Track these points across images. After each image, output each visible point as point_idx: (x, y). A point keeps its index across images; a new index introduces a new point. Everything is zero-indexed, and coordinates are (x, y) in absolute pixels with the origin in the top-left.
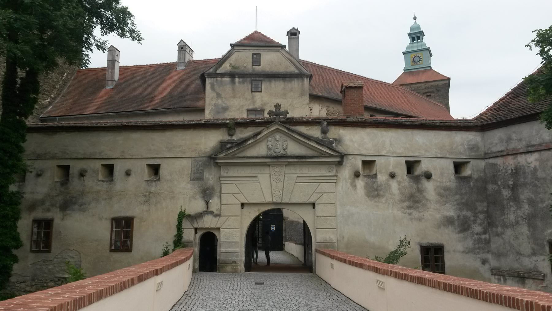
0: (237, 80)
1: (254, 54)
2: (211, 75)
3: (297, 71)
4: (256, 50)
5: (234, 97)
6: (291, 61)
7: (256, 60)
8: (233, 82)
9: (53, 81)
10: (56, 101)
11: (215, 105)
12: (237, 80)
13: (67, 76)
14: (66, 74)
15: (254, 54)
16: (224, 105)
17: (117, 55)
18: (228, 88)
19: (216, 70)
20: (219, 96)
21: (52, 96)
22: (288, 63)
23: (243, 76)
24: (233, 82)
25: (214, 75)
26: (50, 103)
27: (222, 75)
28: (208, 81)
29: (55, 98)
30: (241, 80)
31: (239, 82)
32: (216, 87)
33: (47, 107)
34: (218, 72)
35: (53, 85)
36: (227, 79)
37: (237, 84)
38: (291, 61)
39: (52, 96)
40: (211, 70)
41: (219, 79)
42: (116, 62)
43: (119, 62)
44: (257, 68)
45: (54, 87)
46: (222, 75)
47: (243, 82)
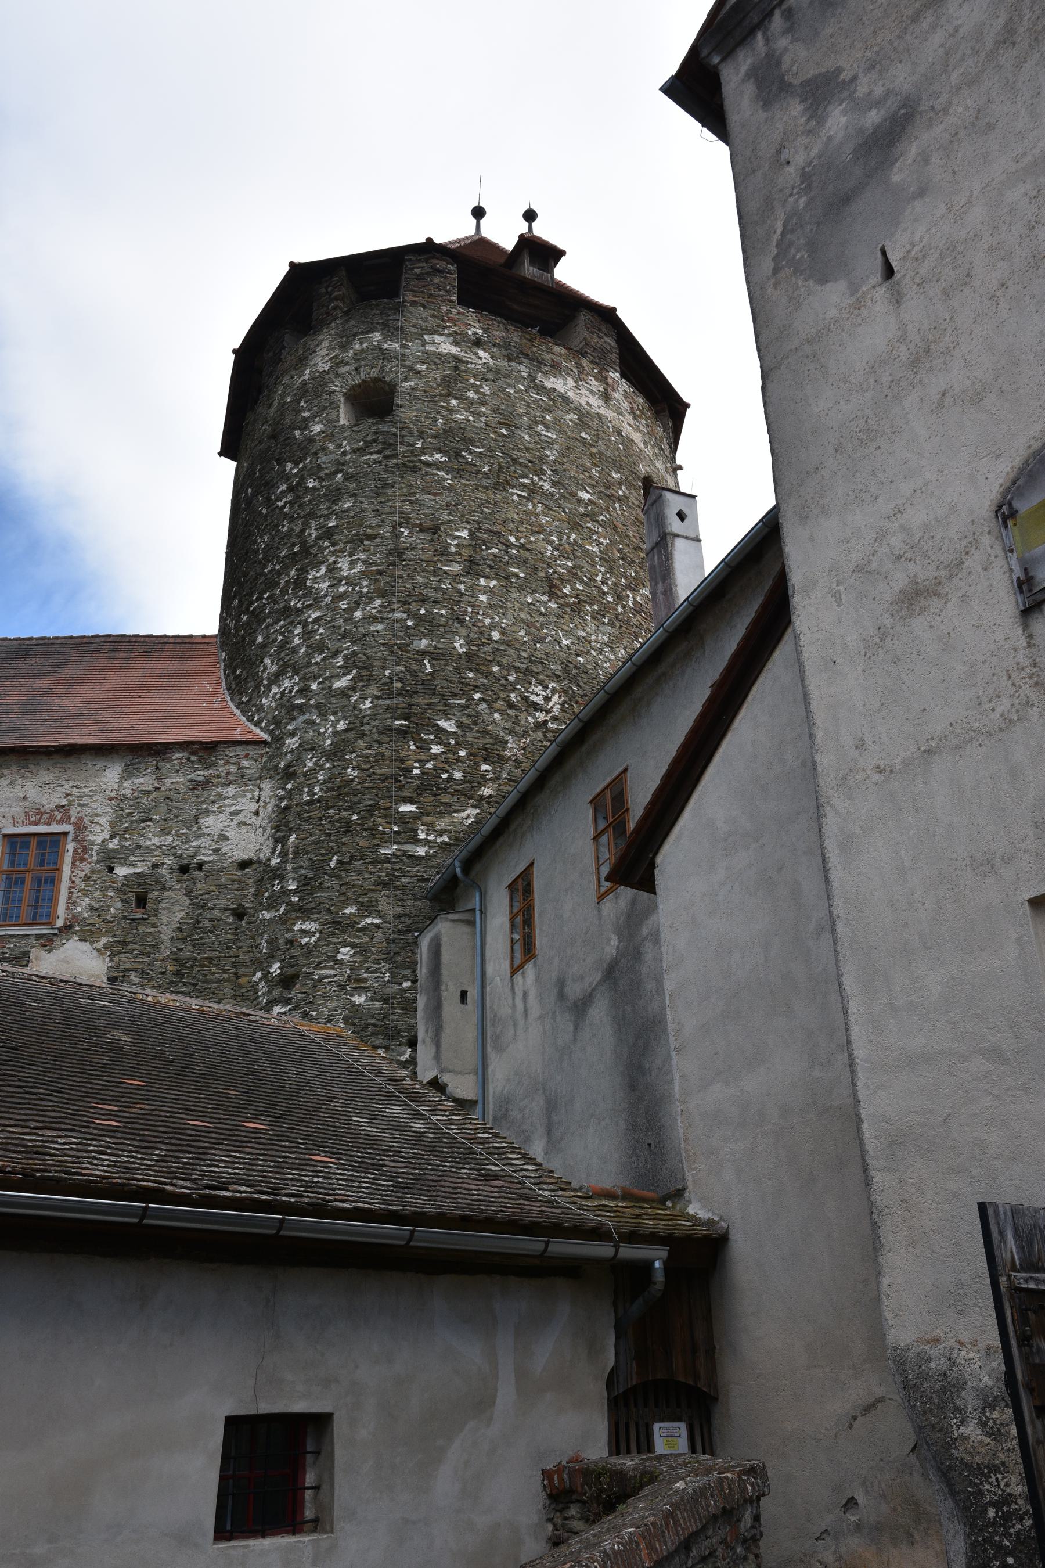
17: (681, 516)
35: (486, 749)
39: (486, 791)
42: (680, 544)
43: (699, 541)
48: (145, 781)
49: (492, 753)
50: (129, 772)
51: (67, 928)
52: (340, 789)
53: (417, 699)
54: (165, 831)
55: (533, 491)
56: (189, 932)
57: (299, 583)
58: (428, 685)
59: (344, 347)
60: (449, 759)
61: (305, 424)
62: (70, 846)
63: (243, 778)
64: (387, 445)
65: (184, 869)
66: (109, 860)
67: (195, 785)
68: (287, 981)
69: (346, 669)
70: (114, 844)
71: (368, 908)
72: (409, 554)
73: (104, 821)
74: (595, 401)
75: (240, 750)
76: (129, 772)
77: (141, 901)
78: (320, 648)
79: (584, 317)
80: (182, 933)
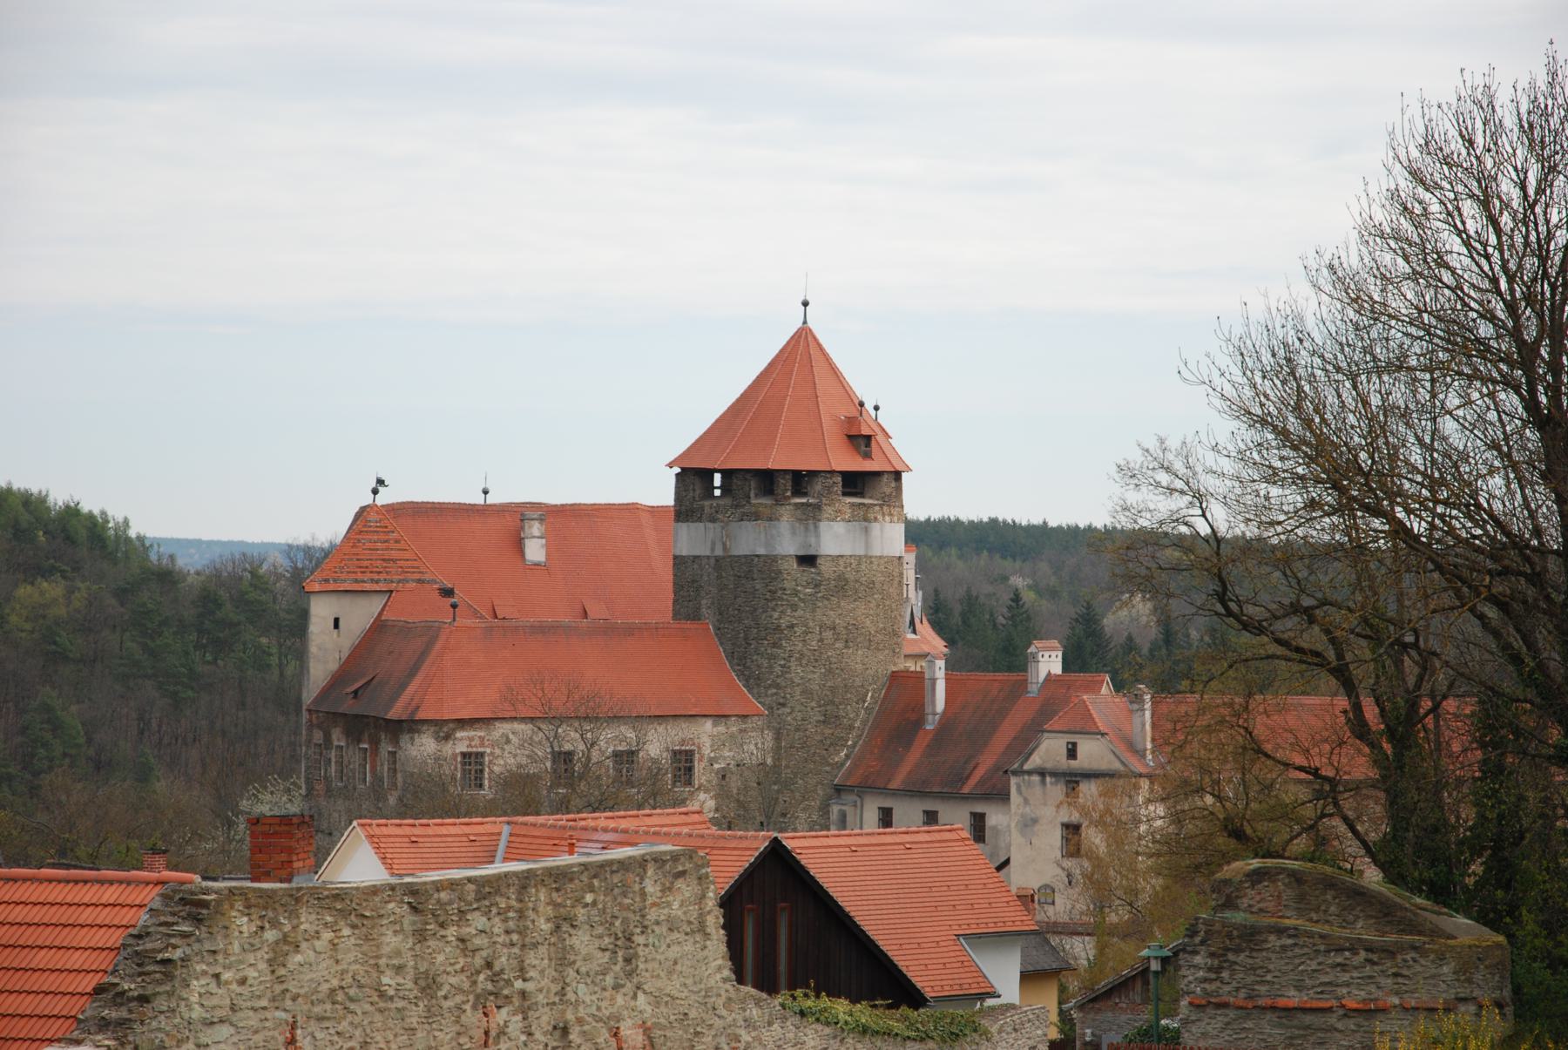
0: (1048, 779)
1: (1068, 743)
2: (1015, 773)
3: (1122, 768)
4: (1073, 738)
5: (1045, 804)
6: (1114, 753)
7: (1072, 753)
8: (1043, 782)
9: (850, 719)
10: (857, 749)
11: (1023, 816)
12: (1048, 779)
13: (872, 698)
14: (870, 695)
15: (1068, 743)
16: (1033, 815)
18: (1038, 790)
19: (1022, 765)
20: (1026, 801)
21: (850, 743)
22: (1112, 757)
23: (1054, 774)
24: (1043, 782)
25: (1019, 772)
26: (847, 756)
27: (1030, 773)
28: (1014, 781)
30: (1053, 780)
31: (1051, 783)
32: (1023, 789)
33: (843, 764)
34: (1026, 767)
36: (1036, 778)
37: (1048, 785)
38: (1114, 753)
40: (1016, 766)
41: (1026, 777)
44: (1072, 762)
45: (851, 727)
46: (1030, 773)
47: (1055, 784)
48: (721, 729)
50: (715, 725)
51: (699, 788)
53: (828, 708)
54: (730, 750)
62: (697, 755)
64: (816, 586)
65: (738, 765)
66: (711, 762)
67: (741, 731)
70: (712, 755)
72: (825, 641)
73: (708, 745)
75: (756, 718)
76: (715, 725)
77: (724, 777)
79: (885, 478)
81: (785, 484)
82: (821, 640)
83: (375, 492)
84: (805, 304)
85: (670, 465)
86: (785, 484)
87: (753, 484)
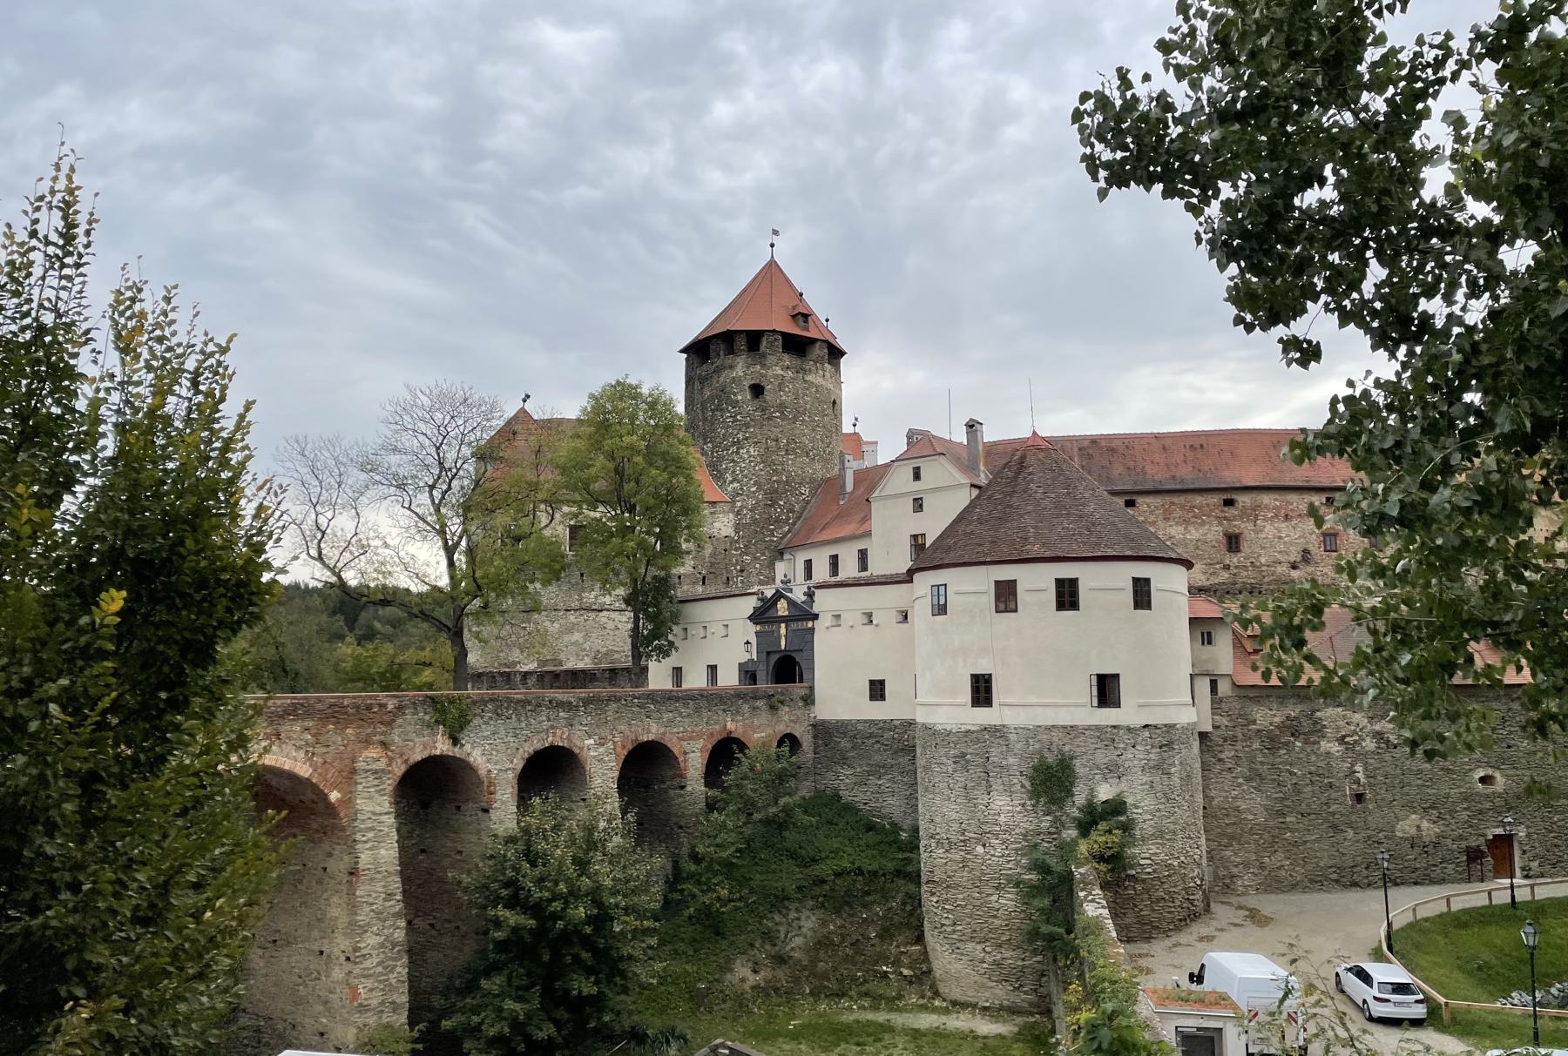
26: (789, 531)
29: (794, 523)
49: (792, 511)
52: (755, 521)
55: (803, 421)
56: (714, 555)
57: (738, 453)
58: (776, 491)
59: (748, 367)
60: (782, 513)
61: (735, 394)
63: (724, 512)
68: (742, 571)
69: (754, 484)
71: (763, 554)
74: (820, 380)
78: (746, 476)
79: (818, 345)
80: (711, 556)
81: (741, 343)
82: (767, 448)
83: (524, 401)
84: (772, 245)
85: (682, 351)
86: (741, 343)
87: (722, 346)
